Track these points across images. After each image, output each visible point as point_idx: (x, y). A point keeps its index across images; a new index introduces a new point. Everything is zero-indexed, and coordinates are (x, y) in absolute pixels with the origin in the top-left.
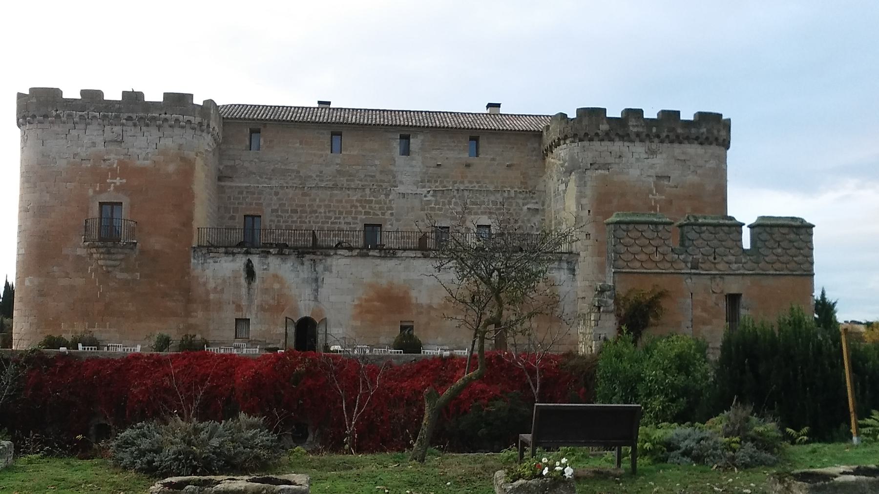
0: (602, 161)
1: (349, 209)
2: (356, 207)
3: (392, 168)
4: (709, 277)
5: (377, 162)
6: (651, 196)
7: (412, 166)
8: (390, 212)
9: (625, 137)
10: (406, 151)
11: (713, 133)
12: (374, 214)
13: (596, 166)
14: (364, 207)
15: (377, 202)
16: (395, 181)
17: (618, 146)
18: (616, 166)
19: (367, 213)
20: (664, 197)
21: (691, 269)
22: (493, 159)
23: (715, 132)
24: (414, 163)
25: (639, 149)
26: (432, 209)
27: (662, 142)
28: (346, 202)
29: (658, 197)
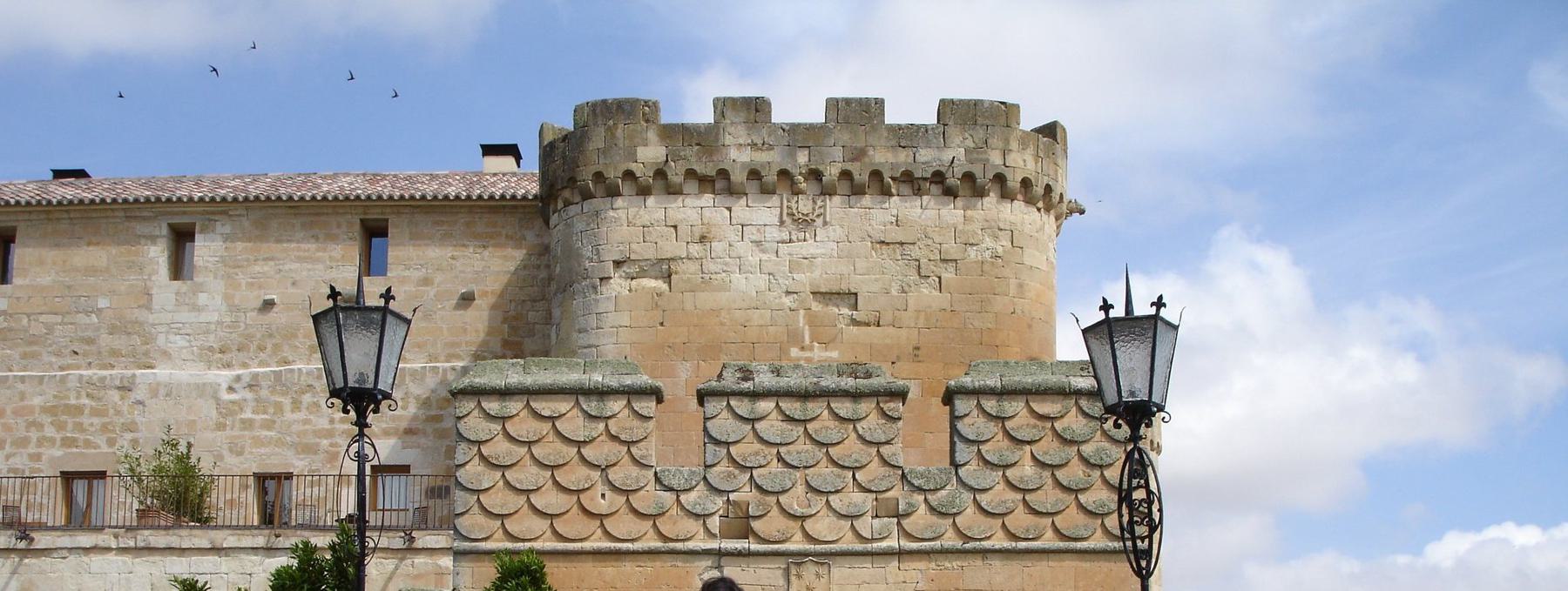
0: (650, 253)
1: (22, 433)
2: (40, 426)
3: (142, 315)
4: (781, 563)
5: (103, 303)
6: (795, 352)
7: (196, 308)
8: (129, 436)
9: (719, 183)
10: (179, 268)
11: (985, 162)
12: (88, 444)
13: (633, 270)
14: (60, 427)
15: (95, 412)
16: (146, 354)
17: (696, 208)
18: (692, 267)
19: (68, 442)
20: (835, 354)
21: (725, 535)
22: (426, 281)
23: (995, 158)
24: (202, 298)
25: (762, 213)
26: (248, 424)
27: (827, 192)
28: (16, 413)
29: (818, 353)
